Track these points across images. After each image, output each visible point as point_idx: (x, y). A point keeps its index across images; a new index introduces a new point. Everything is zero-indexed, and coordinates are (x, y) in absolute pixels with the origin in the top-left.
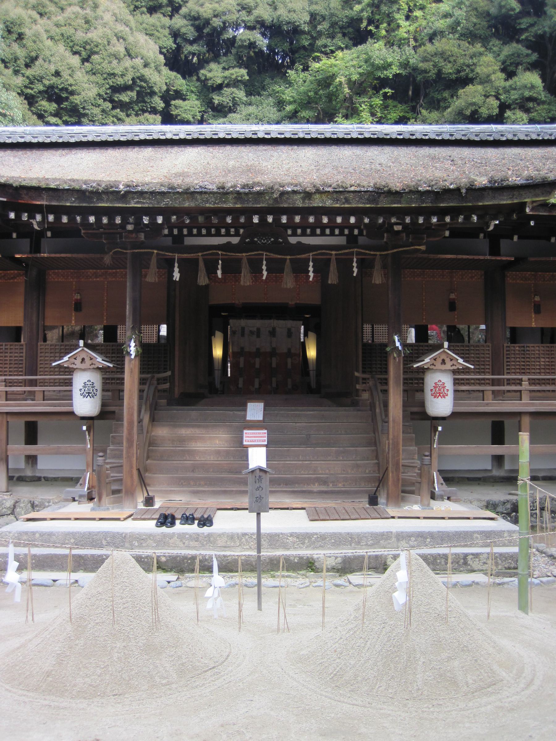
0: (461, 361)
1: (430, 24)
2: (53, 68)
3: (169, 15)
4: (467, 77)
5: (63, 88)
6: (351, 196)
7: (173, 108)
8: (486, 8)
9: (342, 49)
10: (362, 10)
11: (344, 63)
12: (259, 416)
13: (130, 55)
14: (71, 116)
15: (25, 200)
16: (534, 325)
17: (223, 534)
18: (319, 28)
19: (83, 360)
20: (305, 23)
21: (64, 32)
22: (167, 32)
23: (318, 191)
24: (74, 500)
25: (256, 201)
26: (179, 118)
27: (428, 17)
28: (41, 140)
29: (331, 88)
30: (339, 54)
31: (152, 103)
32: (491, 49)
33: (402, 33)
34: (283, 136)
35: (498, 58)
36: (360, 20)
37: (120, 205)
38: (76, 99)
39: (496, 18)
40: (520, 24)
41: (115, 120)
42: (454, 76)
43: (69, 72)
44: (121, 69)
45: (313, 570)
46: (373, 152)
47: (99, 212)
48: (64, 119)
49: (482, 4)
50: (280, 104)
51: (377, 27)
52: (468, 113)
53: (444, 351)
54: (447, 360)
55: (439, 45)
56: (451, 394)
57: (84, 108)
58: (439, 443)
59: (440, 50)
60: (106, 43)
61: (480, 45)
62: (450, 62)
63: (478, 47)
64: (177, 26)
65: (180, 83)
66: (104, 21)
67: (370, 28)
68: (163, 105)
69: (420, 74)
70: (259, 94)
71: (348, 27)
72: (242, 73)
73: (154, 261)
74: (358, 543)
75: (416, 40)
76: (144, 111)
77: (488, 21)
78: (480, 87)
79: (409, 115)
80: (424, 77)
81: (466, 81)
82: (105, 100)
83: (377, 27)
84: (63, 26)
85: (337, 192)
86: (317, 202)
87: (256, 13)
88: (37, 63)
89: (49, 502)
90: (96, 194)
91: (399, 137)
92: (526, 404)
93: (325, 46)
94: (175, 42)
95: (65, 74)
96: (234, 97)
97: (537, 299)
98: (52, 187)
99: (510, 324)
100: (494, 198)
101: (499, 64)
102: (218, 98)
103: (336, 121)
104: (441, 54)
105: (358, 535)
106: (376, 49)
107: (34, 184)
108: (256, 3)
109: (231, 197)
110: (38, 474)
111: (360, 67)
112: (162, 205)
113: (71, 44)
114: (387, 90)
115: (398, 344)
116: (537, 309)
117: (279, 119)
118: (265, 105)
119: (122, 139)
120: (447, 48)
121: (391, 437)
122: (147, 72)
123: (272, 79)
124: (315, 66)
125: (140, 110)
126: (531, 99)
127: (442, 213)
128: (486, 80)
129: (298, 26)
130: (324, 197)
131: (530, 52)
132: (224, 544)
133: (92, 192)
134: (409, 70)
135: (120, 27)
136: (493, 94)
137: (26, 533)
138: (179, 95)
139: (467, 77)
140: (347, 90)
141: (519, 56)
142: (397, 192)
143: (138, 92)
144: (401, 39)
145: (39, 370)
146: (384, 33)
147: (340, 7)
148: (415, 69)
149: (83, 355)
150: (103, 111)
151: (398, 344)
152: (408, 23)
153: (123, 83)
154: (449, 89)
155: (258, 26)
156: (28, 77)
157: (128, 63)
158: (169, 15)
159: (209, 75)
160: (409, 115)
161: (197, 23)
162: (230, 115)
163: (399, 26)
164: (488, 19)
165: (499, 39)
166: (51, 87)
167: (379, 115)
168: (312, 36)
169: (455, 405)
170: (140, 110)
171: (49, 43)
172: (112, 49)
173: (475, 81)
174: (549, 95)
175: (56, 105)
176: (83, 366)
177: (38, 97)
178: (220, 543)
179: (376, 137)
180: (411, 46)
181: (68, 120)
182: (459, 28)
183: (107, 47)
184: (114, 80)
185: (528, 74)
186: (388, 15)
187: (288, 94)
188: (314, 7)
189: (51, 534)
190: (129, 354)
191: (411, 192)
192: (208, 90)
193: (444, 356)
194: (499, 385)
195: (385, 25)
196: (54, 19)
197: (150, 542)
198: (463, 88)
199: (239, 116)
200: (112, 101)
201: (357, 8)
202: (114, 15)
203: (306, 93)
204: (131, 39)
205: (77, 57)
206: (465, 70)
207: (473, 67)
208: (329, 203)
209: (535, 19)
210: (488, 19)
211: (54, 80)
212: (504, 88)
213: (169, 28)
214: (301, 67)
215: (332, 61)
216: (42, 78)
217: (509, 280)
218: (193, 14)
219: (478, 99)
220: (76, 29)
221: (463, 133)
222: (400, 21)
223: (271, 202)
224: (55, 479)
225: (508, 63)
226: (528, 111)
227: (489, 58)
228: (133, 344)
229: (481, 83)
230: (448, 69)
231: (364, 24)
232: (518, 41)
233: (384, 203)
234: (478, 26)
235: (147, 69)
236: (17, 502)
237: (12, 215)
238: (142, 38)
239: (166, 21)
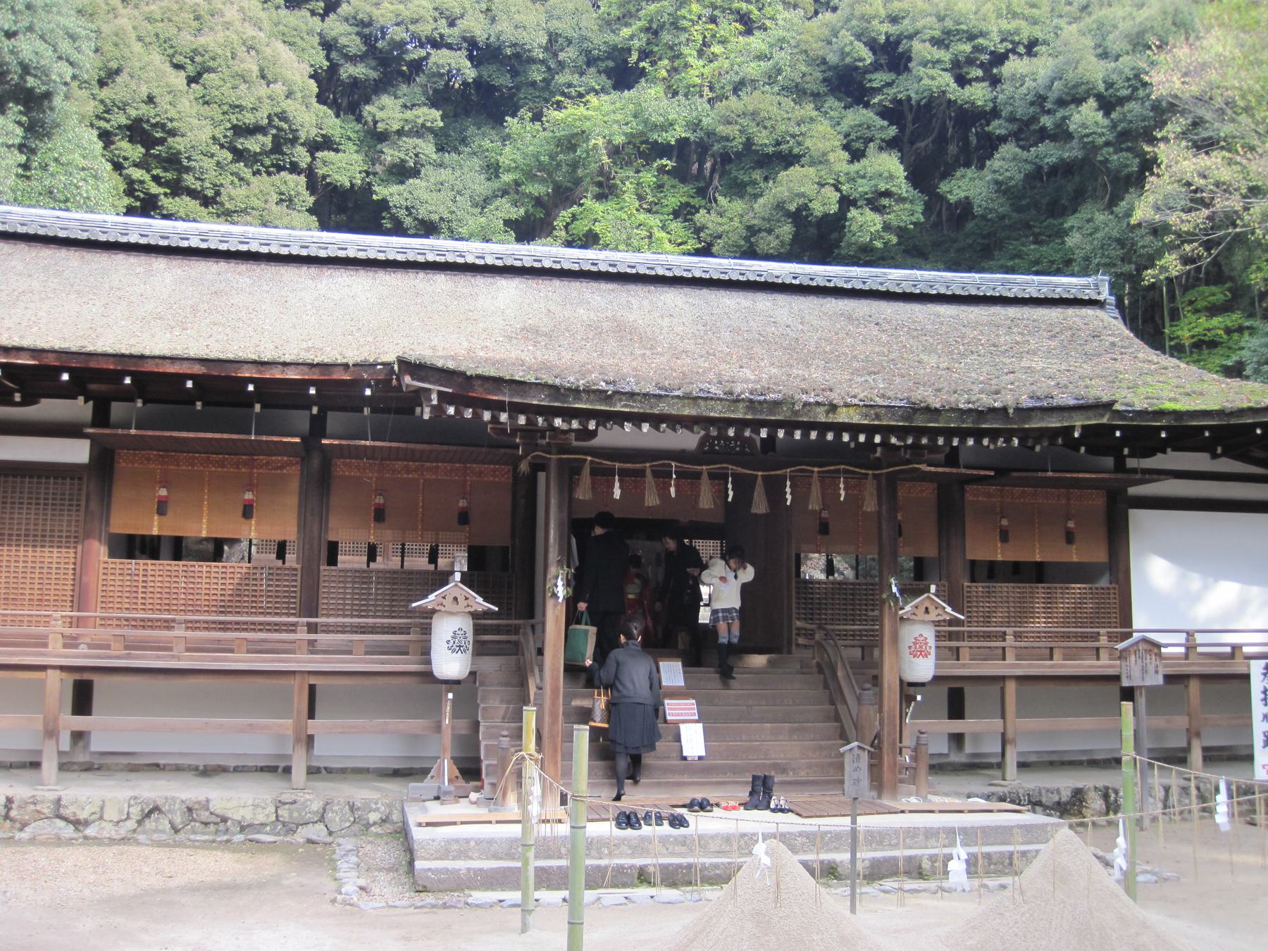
0: (949, 609)
1: (736, 67)
2: (144, 91)
3: (320, 15)
4: (790, 151)
5: (157, 123)
6: (883, 411)
7: (318, 163)
8: (821, 53)
9: (597, 93)
10: (632, 37)
11: (602, 116)
12: (680, 682)
13: (263, 77)
14: (165, 170)
15: (478, 392)
16: (1000, 558)
17: (717, 835)
18: (562, 56)
19: (455, 599)
20: (541, 47)
21: (160, 31)
22: (317, 39)
23: (847, 405)
24: (437, 798)
25: (771, 412)
27: (732, 56)
28: (274, 250)
29: (578, 153)
30: (591, 98)
32: (826, 113)
33: (692, 76)
34: (634, 271)
35: (838, 128)
36: (629, 50)
37: (602, 408)
38: (178, 143)
39: (835, 68)
40: (870, 81)
41: (236, 180)
42: (771, 150)
43: (168, 98)
44: (252, 100)
45: (836, 878)
46: (764, 302)
47: (568, 414)
48: (154, 172)
49: (814, 45)
50: (493, 170)
51: (653, 63)
52: (792, 207)
53: (929, 598)
54: (931, 609)
55: (750, 100)
56: (933, 651)
57: (189, 158)
58: (912, 718)
59: (750, 108)
60: (229, 55)
61: (812, 106)
62: (765, 128)
63: (809, 109)
64: (334, 34)
65: (333, 125)
66: (226, 19)
67: (642, 64)
68: (309, 159)
70: (456, 150)
71: (607, 58)
72: (434, 116)
73: (587, 470)
74: (880, 843)
75: (711, 89)
76: (280, 169)
77: (824, 72)
78: (811, 171)
79: (696, 202)
80: (724, 147)
81: (789, 160)
82: (222, 146)
83: (653, 63)
84: (157, 21)
85: (866, 406)
86: (843, 416)
87: (462, 24)
88: (119, 79)
89: (376, 803)
90: (576, 392)
91: (794, 282)
92: (1011, 666)
93: (570, 85)
94: (328, 58)
95: (163, 101)
97: (1005, 522)
98: (517, 378)
99: (970, 557)
100: (1042, 419)
101: (842, 137)
102: (391, 152)
103: (582, 205)
104: (752, 114)
105: (880, 833)
106: (650, 96)
107: (492, 372)
108: (464, 8)
109: (741, 405)
110: (315, 764)
111: (627, 124)
112: (656, 411)
113: (171, 51)
114: (665, 161)
115: (894, 589)
116: (1004, 536)
117: (490, 192)
118: (466, 169)
119: (400, 258)
120: (761, 106)
121: (886, 708)
122: (291, 107)
123: (479, 129)
124: (553, 115)
125: (273, 165)
126: (887, 194)
127: (979, 434)
128: (820, 161)
129: (529, 51)
130: (851, 410)
131: (886, 123)
132: (717, 849)
133: (569, 389)
134: (700, 134)
135: (250, 31)
136: (832, 182)
137: (457, 841)
138: (327, 143)
139: (790, 151)
140: (606, 159)
141: (869, 127)
142: (936, 409)
143: (274, 136)
144: (688, 87)
145: (321, 606)
146: (664, 73)
147: (596, 27)
148: (710, 134)
149: (457, 593)
150: (218, 163)
151: (894, 589)
152: (701, 63)
153: (253, 121)
154: (762, 167)
155: (465, 45)
156: (102, 102)
157: (263, 90)
158: (320, 15)
159: (380, 115)
160: (696, 202)
161: (367, 31)
162: (411, 181)
163: (687, 65)
164: (823, 67)
165: (840, 100)
166: (138, 121)
167: (650, 198)
168: (549, 69)
169: (937, 666)
170: (273, 165)
171: (138, 47)
172: (238, 67)
173: (803, 160)
174: (911, 189)
175: (143, 150)
176: (455, 608)
177: (116, 135)
178: (713, 847)
179: (762, 279)
180: (706, 98)
181: (162, 175)
182: (780, 78)
183: (231, 62)
184: (240, 116)
185: (884, 155)
186: (671, 48)
187: (508, 156)
188: (555, 25)
189: (490, 842)
190: (555, 595)
191: (952, 410)
192: (376, 137)
193: (927, 604)
194: (958, 640)
195: (666, 62)
196: (147, 9)
197: (624, 848)
198: (786, 168)
199: (424, 184)
200: (233, 150)
201: (626, 32)
202: (241, 10)
203: (536, 156)
204: (268, 51)
205: (183, 74)
207: (800, 139)
208: (856, 419)
209: (893, 76)
210: (823, 67)
211: (145, 110)
212: (847, 174)
213: (320, 34)
214: (530, 114)
215: (582, 110)
216: (126, 104)
217: (969, 497)
218: (360, 16)
219: (809, 189)
220: (179, 29)
221: (879, 280)
222: (690, 60)
223: (789, 414)
224: (343, 771)
225: (853, 136)
226: (878, 209)
227: (823, 127)
228: (560, 583)
229: (812, 164)
230: (763, 139)
231: (634, 57)
232: (867, 105)
233: (919, 422)
234: (808, 78)
235: (289, 101)
236: (327, 804)
237: (451, 410)
238: (285, 53)
239: (316, 23)
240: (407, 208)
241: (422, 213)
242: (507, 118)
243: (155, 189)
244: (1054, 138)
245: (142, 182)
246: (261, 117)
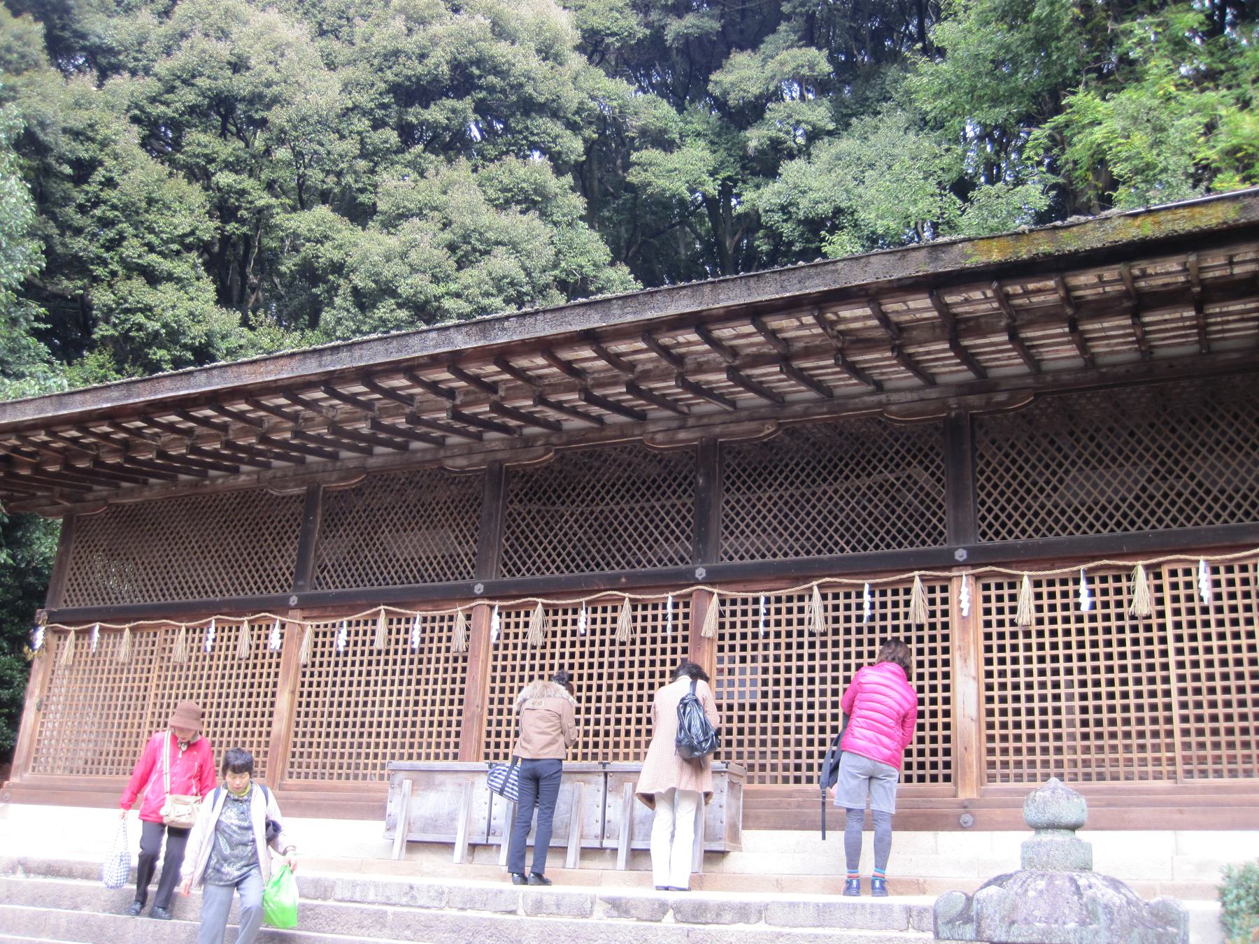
26: (649, 191)
31: (532, 134)
72: (818, 60)
240: (784, 209)
241: (804, 206)
243: (263, 199)
245: (243, 192)
246: (439, 63)
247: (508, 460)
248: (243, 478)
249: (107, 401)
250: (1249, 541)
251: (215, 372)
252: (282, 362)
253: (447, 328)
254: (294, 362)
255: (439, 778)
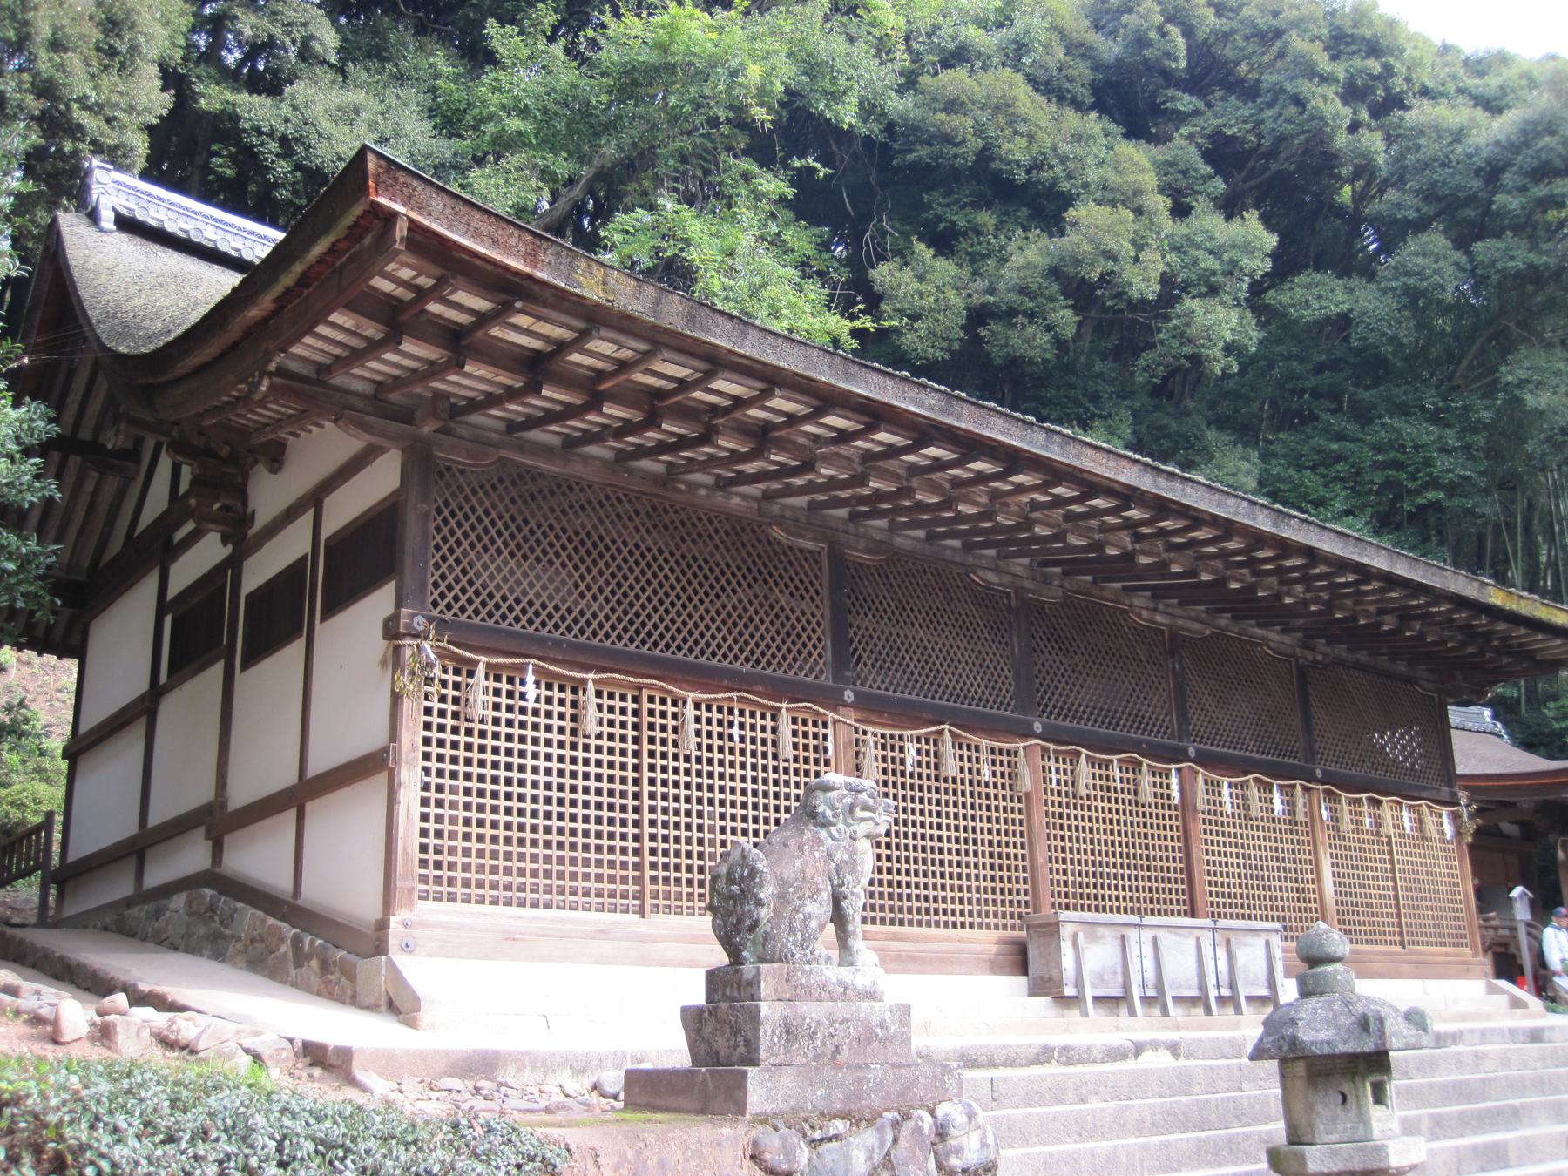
69: (929, 144)
96: (312, 37)
102: (252, 19)
206: (1051, 167)
230: (1015, 150)
240: (284, 141)
242: (491, 27)
244: (1518, 229)
247: (1033, 592)
248: (736, 500)
249: (920, 404)
250: (1415, 794)
251: (1056, 438)
252: (1124, 463)
253: (1255, 503)
254: (1135, 469)
255: (1101, 930)
